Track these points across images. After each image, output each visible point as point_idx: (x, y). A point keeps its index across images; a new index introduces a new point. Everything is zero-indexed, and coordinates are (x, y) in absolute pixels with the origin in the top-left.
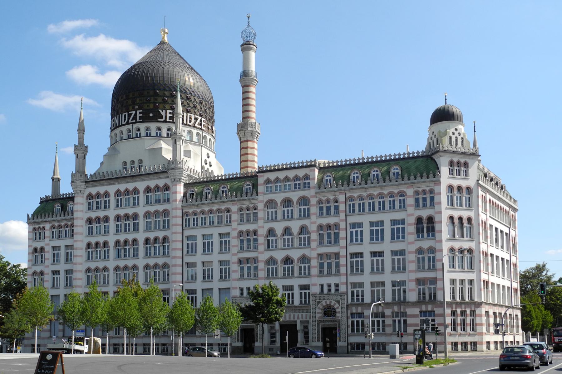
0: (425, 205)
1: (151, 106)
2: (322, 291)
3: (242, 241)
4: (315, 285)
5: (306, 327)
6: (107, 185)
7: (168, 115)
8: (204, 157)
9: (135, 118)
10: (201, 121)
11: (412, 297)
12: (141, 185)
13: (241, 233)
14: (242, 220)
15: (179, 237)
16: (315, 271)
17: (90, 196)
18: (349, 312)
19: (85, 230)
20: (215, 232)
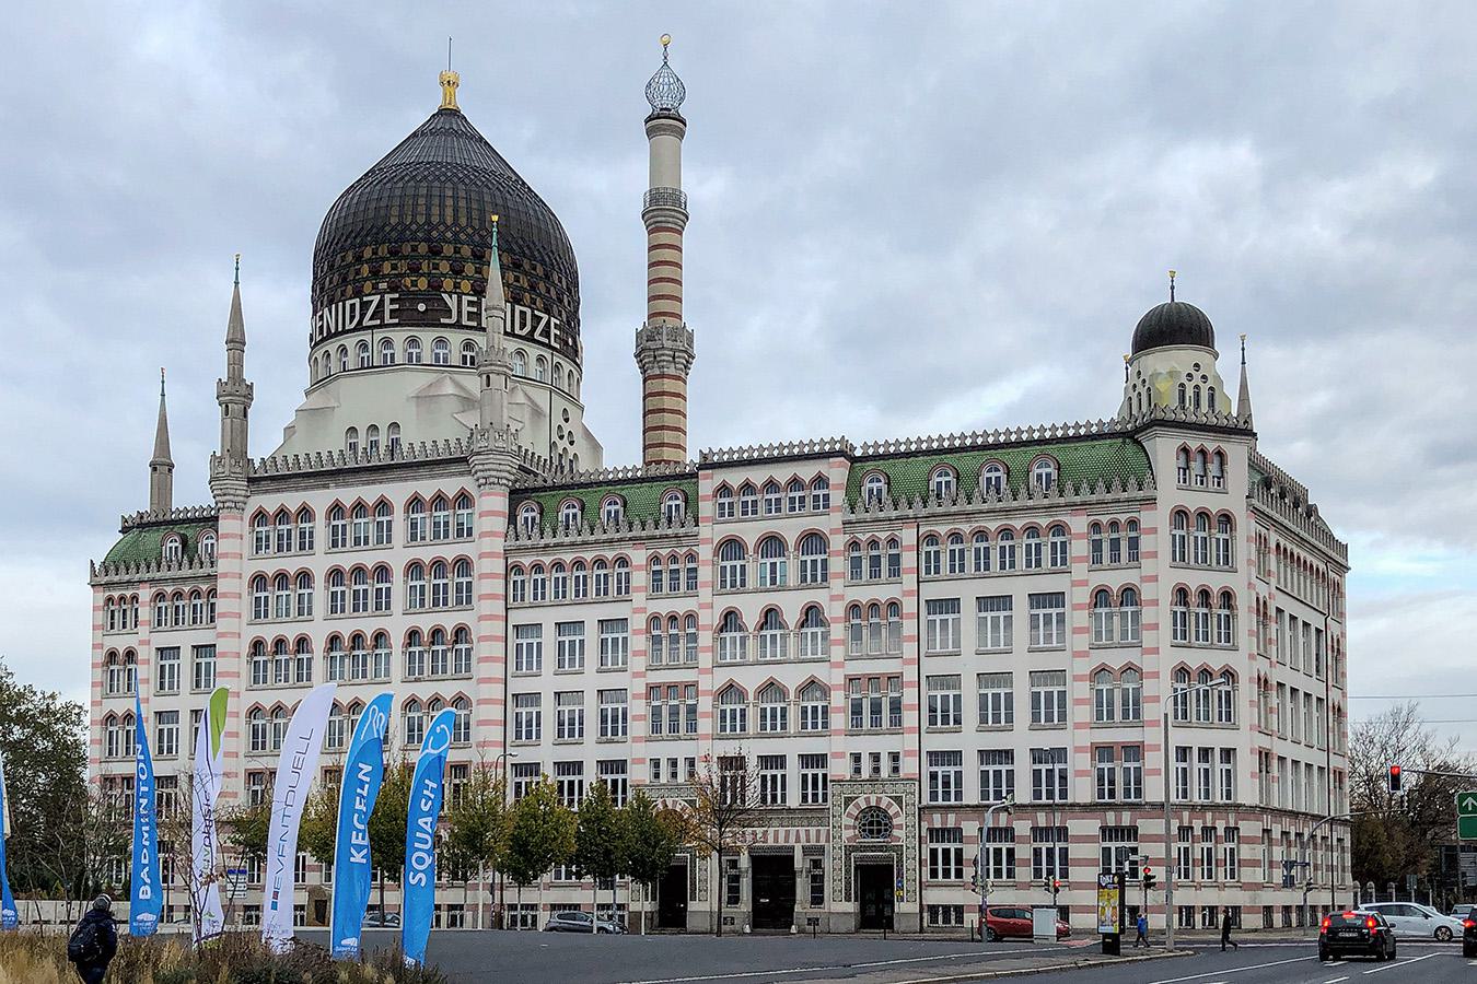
0: (1116, 558)
1: (423, 284)
2: (858, 771)
3: (657, 640)
4: (841, 755)
5: (817, 864)
6: (306, 489)
7: (466, 309)
8: (558, 420)
9: (378, 313)
10: (549, 322)
11: (1082, 790)
12: (398, 492)
13: (655, 619)
14: (657, 587)
15: (497, 628)
16: (839, 721)
17: (260, 516)
18: (925, 825)
19: (245, 606)
20: (591, 615)
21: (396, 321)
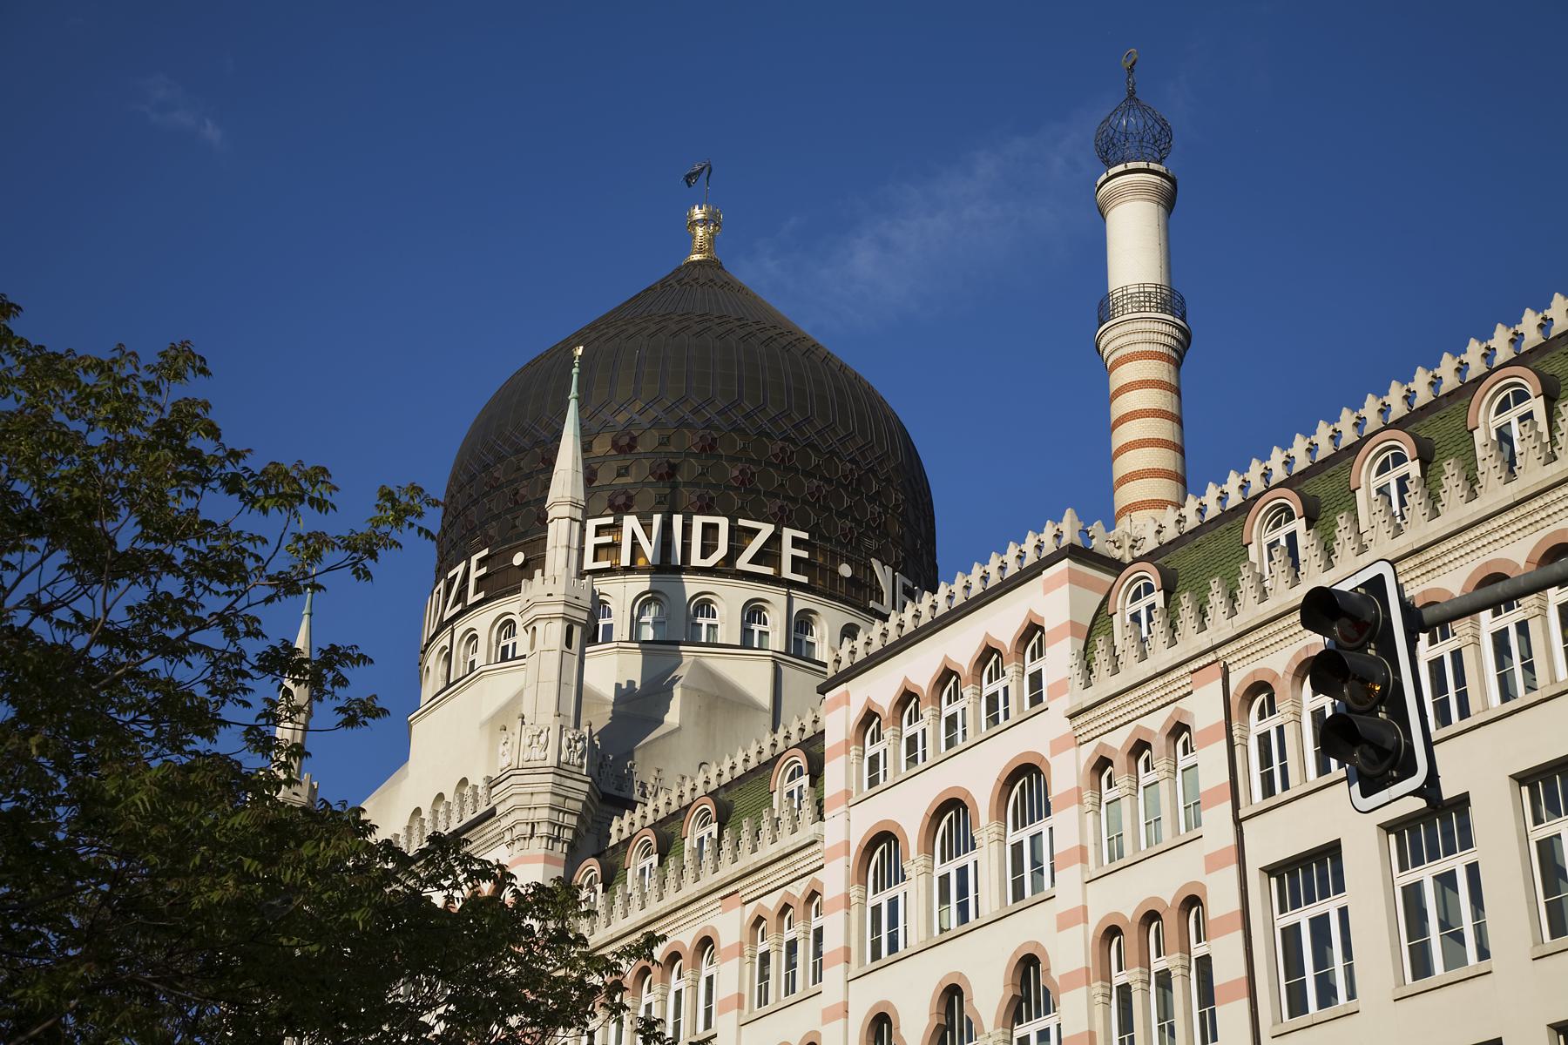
9: (770, 553)
21: (804, 579)
